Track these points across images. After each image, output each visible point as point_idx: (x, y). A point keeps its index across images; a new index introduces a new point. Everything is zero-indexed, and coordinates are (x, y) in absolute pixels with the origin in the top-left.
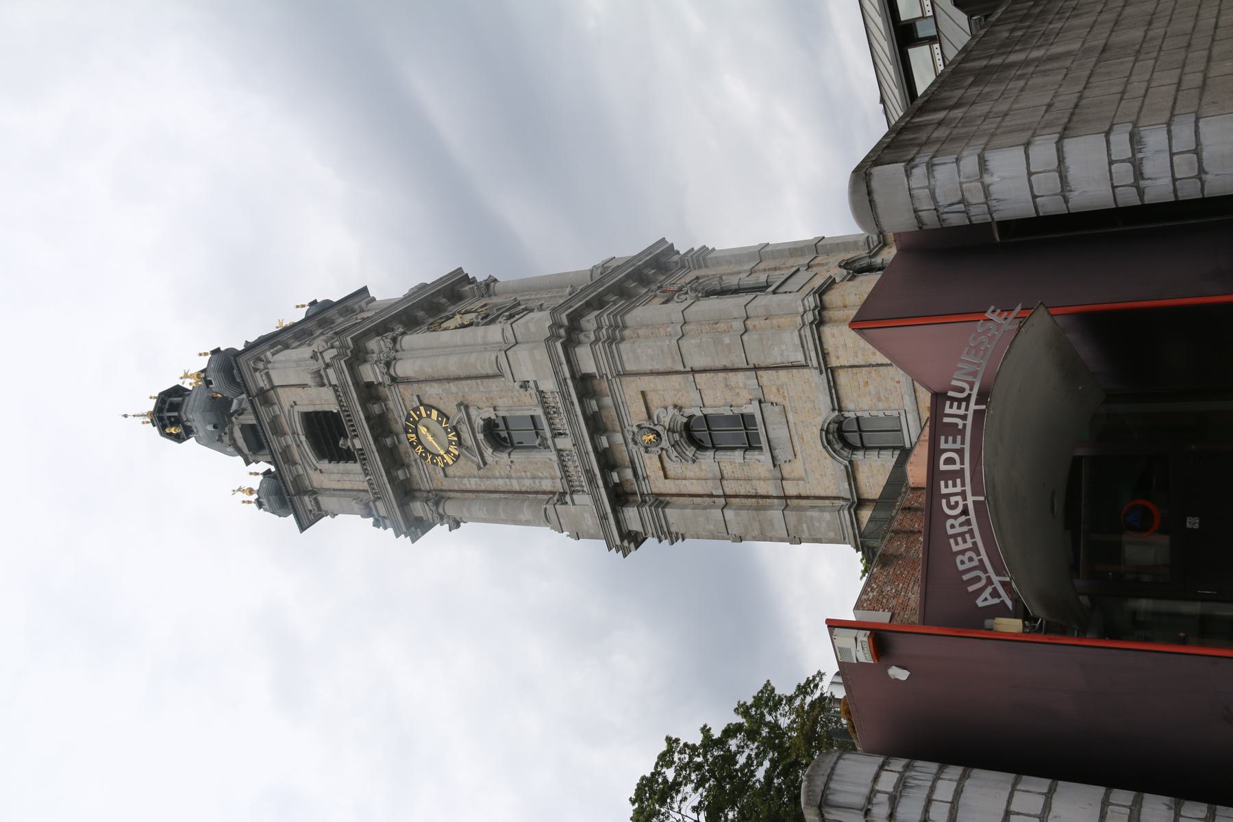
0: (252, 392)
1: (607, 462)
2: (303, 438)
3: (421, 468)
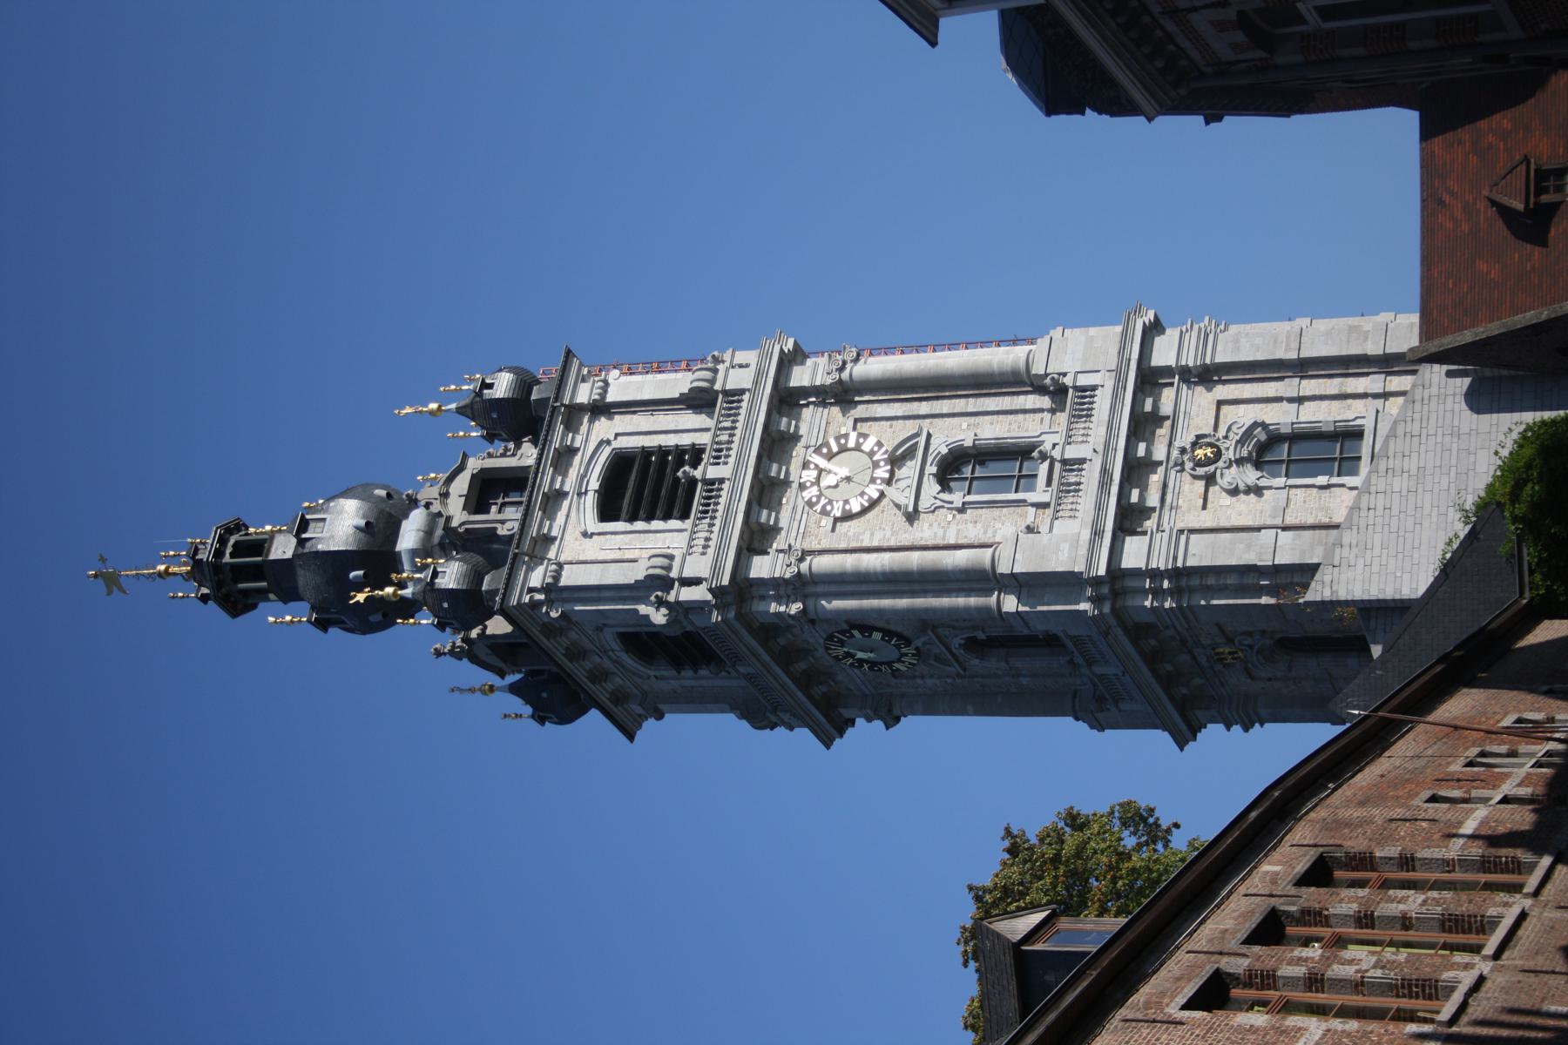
0: (563, 398)
1: (1136, 470)
2: (594, 484)
3: (798, 517)
